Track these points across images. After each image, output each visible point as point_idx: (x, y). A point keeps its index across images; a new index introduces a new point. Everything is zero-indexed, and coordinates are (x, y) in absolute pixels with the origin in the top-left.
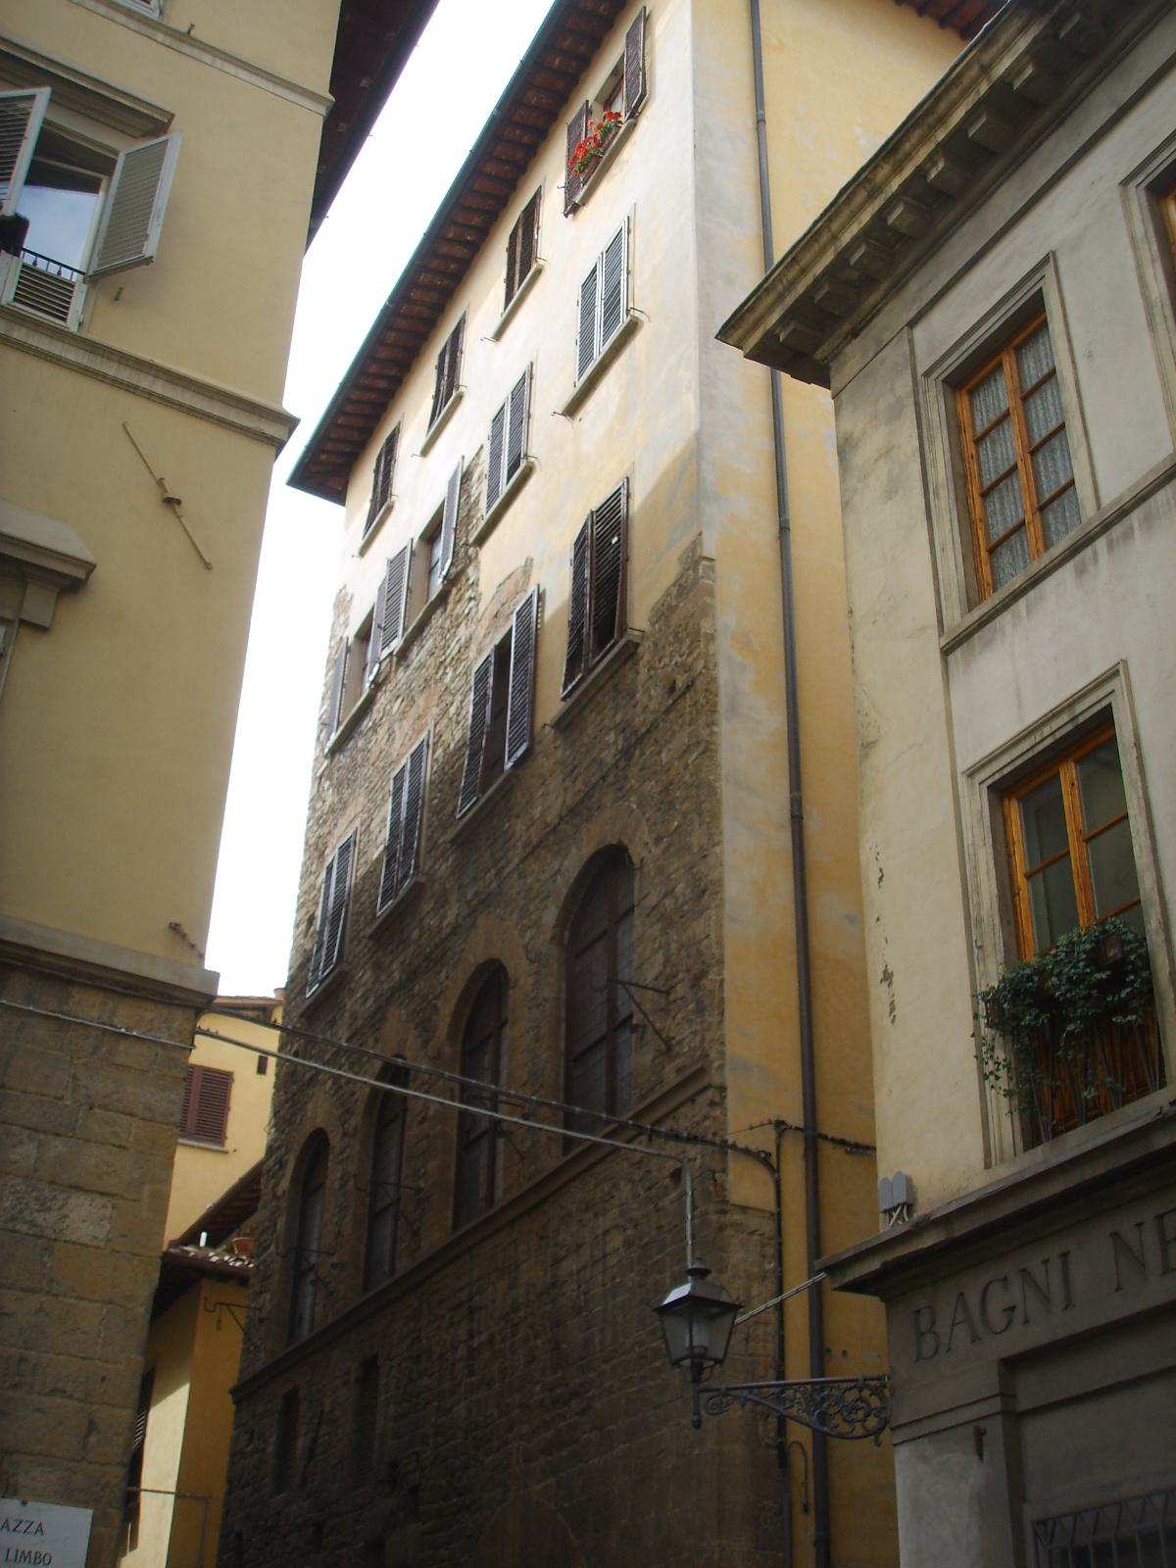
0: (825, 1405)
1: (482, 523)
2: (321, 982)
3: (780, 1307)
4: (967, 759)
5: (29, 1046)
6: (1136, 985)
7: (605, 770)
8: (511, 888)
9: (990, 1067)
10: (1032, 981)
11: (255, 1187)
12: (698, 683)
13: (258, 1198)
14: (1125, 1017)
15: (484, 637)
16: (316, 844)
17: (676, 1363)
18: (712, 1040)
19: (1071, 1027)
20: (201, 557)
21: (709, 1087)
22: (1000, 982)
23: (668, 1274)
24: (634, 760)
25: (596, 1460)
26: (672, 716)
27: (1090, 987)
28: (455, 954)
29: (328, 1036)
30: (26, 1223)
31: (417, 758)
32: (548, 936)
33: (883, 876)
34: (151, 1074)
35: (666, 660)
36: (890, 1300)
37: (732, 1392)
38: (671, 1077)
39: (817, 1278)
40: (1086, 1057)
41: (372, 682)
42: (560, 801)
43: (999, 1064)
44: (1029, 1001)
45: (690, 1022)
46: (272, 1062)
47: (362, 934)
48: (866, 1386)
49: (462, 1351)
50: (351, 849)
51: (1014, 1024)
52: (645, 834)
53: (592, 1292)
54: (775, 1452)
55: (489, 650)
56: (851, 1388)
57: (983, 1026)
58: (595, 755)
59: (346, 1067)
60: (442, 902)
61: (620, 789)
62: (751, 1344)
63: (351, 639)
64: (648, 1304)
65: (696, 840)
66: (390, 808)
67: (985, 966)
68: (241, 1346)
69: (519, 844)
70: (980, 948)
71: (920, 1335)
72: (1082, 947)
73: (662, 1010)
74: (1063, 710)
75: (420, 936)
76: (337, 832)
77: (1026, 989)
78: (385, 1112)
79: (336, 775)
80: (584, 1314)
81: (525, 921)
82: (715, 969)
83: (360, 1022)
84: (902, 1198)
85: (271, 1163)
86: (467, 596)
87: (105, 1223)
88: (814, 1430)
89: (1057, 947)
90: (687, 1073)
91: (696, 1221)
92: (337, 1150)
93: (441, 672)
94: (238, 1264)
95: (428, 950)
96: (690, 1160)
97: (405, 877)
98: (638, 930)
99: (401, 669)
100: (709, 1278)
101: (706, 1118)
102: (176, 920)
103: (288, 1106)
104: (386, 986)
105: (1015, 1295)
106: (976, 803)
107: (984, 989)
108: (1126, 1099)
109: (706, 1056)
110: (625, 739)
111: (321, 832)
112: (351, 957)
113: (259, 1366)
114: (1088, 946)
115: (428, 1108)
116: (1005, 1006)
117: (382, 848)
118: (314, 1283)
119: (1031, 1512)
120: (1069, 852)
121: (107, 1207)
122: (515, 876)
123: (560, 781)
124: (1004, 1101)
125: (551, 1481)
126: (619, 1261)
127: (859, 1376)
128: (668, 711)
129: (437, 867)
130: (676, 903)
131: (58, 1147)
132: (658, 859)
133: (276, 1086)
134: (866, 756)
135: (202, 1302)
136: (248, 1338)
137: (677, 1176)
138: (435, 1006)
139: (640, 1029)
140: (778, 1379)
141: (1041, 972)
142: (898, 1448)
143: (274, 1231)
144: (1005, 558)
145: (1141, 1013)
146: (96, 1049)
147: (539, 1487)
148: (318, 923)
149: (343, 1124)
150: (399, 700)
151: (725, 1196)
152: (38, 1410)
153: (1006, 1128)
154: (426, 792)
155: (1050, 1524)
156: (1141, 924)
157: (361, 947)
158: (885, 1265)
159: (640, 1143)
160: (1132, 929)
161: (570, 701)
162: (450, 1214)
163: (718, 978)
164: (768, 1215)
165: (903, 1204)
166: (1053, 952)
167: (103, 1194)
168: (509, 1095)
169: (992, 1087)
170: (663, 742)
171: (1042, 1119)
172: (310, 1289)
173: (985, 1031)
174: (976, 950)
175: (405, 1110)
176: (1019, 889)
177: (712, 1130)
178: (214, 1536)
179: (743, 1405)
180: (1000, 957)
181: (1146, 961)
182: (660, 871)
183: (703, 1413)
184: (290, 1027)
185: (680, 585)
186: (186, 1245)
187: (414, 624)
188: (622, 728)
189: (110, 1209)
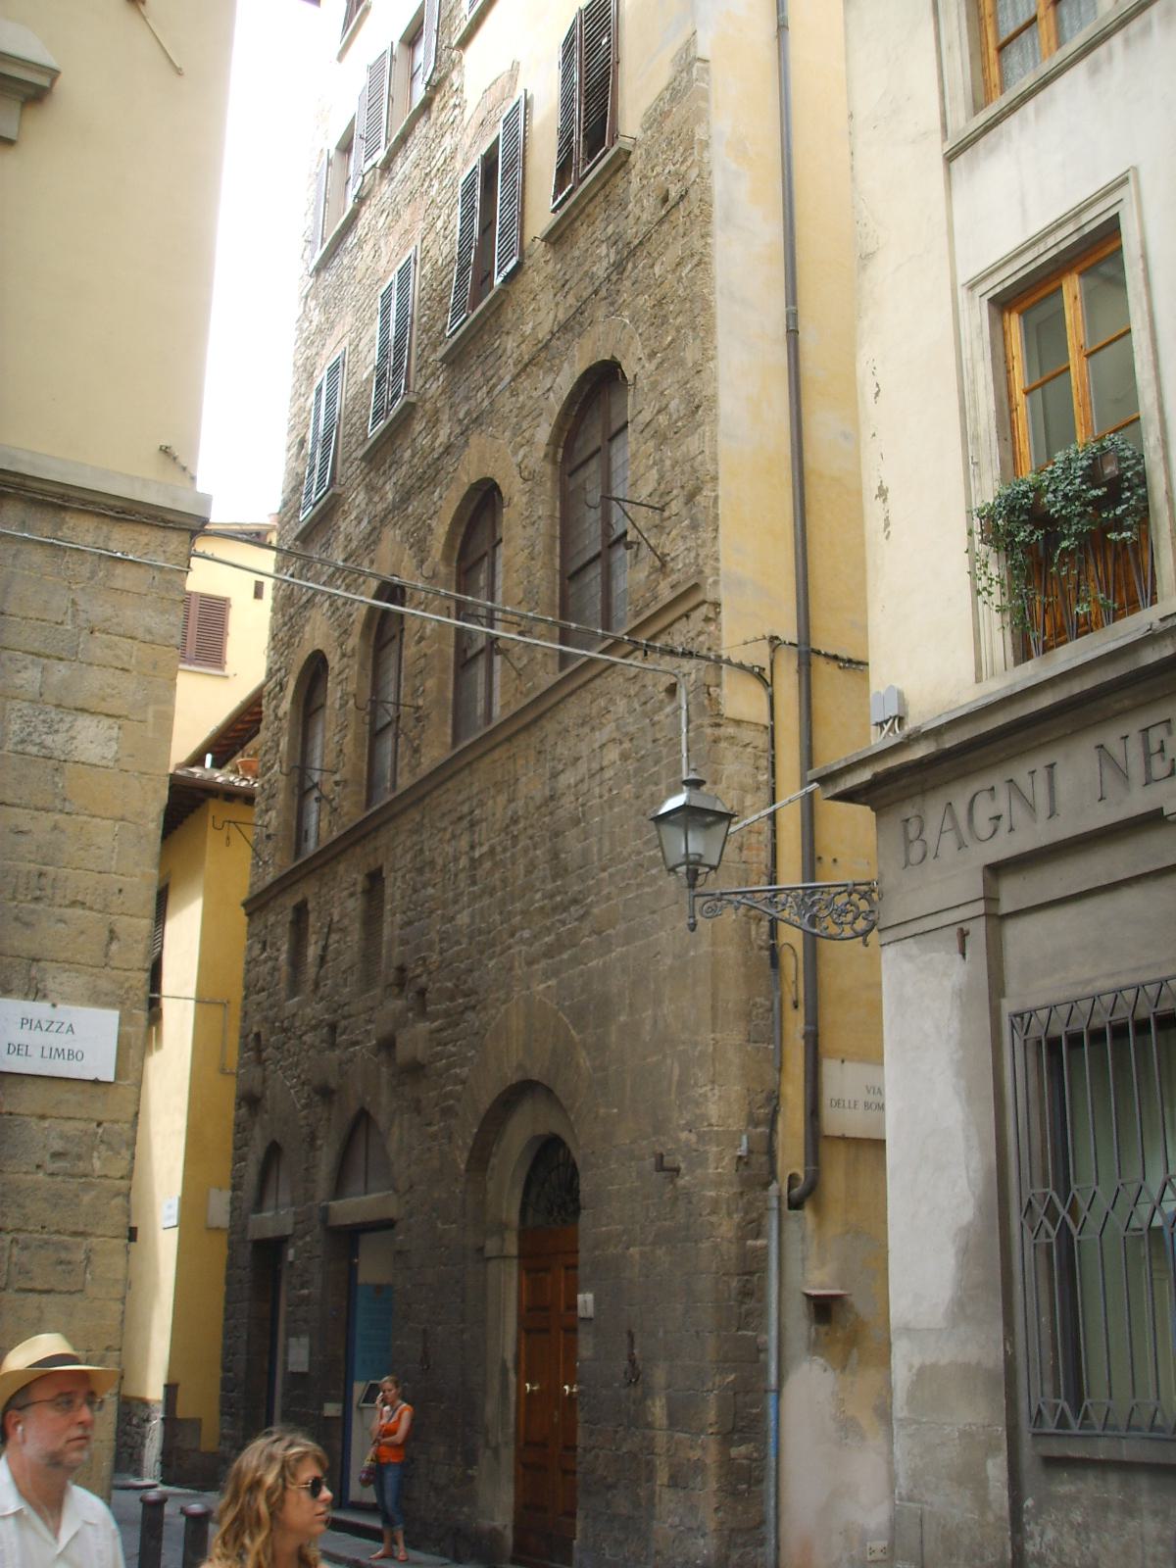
0: (815, 909)
1: (465, 24)
2: (314, 505)
3: (773, 817)
4: (968, 271)
5: (26, 572)
6: (1132, 502)
7: (597, 284)
8: (503, 407)
9: (983, 583)
10: (1028, 497)
11: (256, 709)
12: (691, 192)
13: (260, 721)
14: (1120, 534)
15: (471, 147)
16: (304, 365)
17: (672, 870)
18: (707, 556)
19: (1064, 544)
20: (171, 61)
21: (704, 602)
22: (995, 498)
23: (663, 786)
24: (626, 274)
25: (594, 963)
26: (665, 227)
27: (1085, 504)
28: (449, 473)
29: (324, 556)
30: (35, 745)
31: (404, 274)
32: (542, 455)
33: (879, 391)
34: (149, 598)
35: (658, 169)
36: (879, 810)
37: (726, 897)
38: (666, 594)
39: (810, 788)
40: (1079, 573)
41: (356, 196)
42: (551, 316)
43: (992, 580)
44: (1024, 517)
45: (684, 538)
46: (269, 584)
47: (354, 456)
48: (855, 891)
49: (463, 862)
50: (340, 369)
51: (1008, 540)
52: (638, 349)
53: (590, 804)
54: (767, 953)
55: (476, 160)
56: (840, 894)
57: (977, 542)
58: (586, 269)
59: (343, 587)
60: (434, 422)
61: (612, 304)
62: (745, 852)
63: (333, 152)
64: (644, 814)
65: (690, 355)
66: (379, 326)
67: (981, 484)
68: (250, 861)
69: (510, 361)
70: (976, 464)
71: (908, 842)
72: (1079, 464)
73: (656, 527)
74: (1069, 219)
75: (413, 456)
76: (325, 352)
77: (1021, 506)
78: (382, 631)
79: (322, 294)
80: (583, 824)
81: (519, 439)
82: (709, 486)
83: (354, 544)
84: (894, 712)
85: (271, 684)
86: (451, 103)
87: (113, 743)
88: (804, 931)
89: (1054, 464)
90: (681, 590)
91: (691, 734)
92: (336, 671)
93: (426, 184)
94: (244, 784)
95: (421, 470)
96: (684, 675)
97: (395, 397)
98: (632, 447)
99: (385, 182)
100: (704, 789)
101: (700, 633)
102: (165, 443)
103: (286, 628)
104: (380, 507)
105: (1002, 804)
106: (977, 316)
107: (980, 505)
108: (1116, 616)
109: (701, 572)
110: (617, 253)
111: (309, 353)
112: (344, 479)
113: (269, 879)
114: (1085, 463)
115: (425, 628)
116: (1000, 522)
117: (371, 367)
118: (318, 800)
119: (1008, 1006)
120: (1069, 368)
121: (112, 728)
122: (507, 394)
123: (551, 296)
124: (997, 616)
125: (552, 982)
126: (616, 774)
127: (849, 882)
128: (661, 222)
129: (427, 386)
130: (670, 418)
131: (61, 671)
132: (651, 375)
133: (274, 610)
134: (864, 268)
135: (210, 820)
136: (257, 854)
137: (672, 690)
138: (429, 525)
139: (635, 547)
140: (770, 884)
141: (1037, 489)
142: (886, 947)
143: (278, 751)
144: (1014, 55)
145: (1135, 530)
146: (93, 574)
147: (542, 986)
148: (309, 446)
149: (341, 645)
150: (385, 215)
151: (719, 710)
152: (60, 921)
153: (998, 641)
154: (414, 308)
155: (1027, 1016)
156: (1139, 440)
157: (353, 469)
158: (875, 775)
159: (635, 658)
160: (1131, 445)
161: (561, 213)
162: (449, 731)
163: (713, 494)
164: (762, 728)
165: (895, 717)
166: (1049, 468)
167: (108, 716)
168: (505, 612)
169: (985, 602)
170: (655, 255)
171: (1032, 636)
172: (314, 806)
173: (980, 548)
174: (972, 466)
175: (402, 630)
176: (1017, 405)
177: (707, 645)
178: (234, 1038)
179: (737, 909)
180: (997, 472)
181: (1143, 479)
182: (654, 385)
183: (698, 917)
184: (285, 548)
185: (673, 89)
186: (192, 766)
187: (397, 133)
188: (614, 241)
189: (116, 730)
